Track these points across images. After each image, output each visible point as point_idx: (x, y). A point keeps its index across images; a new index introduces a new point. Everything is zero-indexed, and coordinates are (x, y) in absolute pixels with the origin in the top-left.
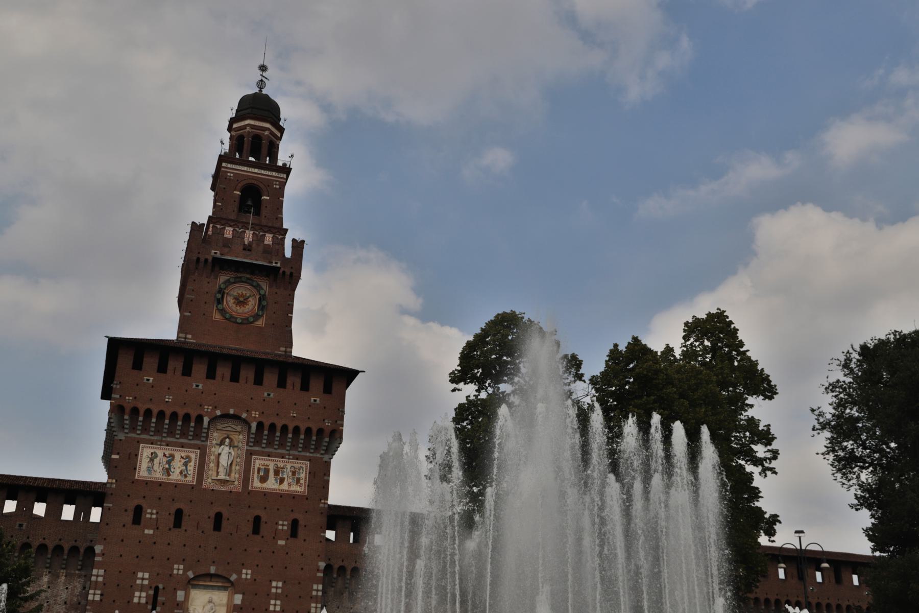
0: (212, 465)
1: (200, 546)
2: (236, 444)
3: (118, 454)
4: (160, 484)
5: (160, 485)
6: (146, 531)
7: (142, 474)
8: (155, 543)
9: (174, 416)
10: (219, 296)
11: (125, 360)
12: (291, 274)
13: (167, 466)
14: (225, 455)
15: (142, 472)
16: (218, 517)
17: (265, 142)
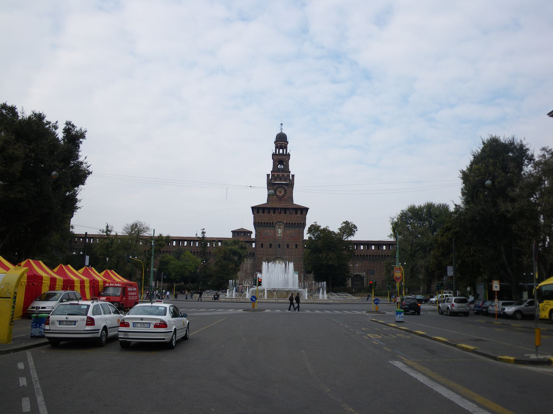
11: (255, 211)
12: (292, 184)
14: (280, 231)
16: (279, 244)
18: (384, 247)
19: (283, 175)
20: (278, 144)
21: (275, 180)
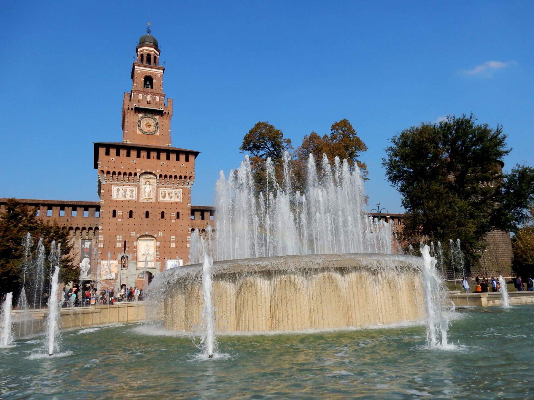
0: (142, 192)
6: (119, 220)
7: (114, 197)
10: (139, 123)
15: (114, 197)
16: (147, 213)
17: (152, 57)
20: (143, 51)
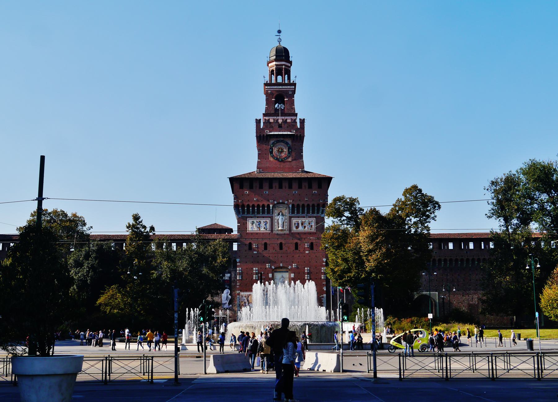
0: (276, 224)
1: (275, 256)
2: (284, 214)
3: (239, 223)
4: (257, 233)
5: (257, 234)
6: (254, 252)
8: (258, 256)
9: (258, 206)
10: (271, 150)
11: (237, 186)
12: (300, 135)
13: (259, 226)
18: (451, 246)
19: (285, 122)
21: (272, 128)
